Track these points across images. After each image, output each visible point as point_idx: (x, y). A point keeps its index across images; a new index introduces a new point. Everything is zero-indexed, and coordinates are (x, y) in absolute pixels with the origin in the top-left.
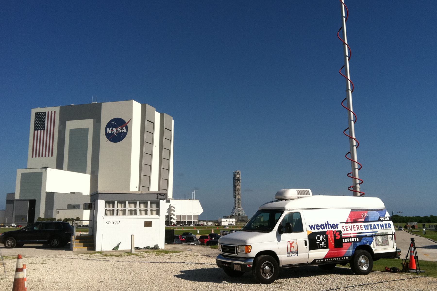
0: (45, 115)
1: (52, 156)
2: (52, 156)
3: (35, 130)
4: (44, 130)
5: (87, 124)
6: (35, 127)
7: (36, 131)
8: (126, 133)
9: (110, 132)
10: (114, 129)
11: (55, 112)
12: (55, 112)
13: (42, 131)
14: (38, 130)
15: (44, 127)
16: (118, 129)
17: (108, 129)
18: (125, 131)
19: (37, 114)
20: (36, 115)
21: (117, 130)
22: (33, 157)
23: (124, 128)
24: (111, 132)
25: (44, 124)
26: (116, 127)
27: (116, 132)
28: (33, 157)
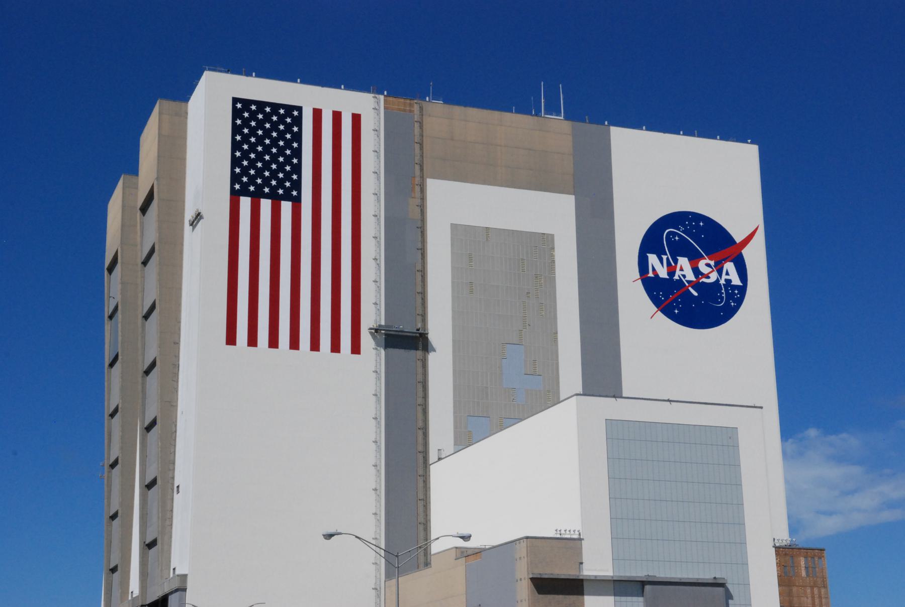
0: (298, 121)
1: (356, 348)
2: (356, 348)
3: (235, 196)
4: (297, 202)
5: (553, 214)
6: (235, 178)
7: (245, 203)
8: (743, 290)
9: (663, 273)
10: (683, 262)
11: (356, 119)
12: (356, 119)
13: (286, 207)
14: (256, 197)
15: (297, 185)
16: (702, 266)
17: (653, 259)
18: (736, 281)
19: (242, 109)
20: (236, 113)
21: (696, 271)
22: (231, 339)
23: (729, 266)
24: (671, 273)
25: (297, 169)
26: (694, 258)
27: (691, 276)
28: (231, 339)
